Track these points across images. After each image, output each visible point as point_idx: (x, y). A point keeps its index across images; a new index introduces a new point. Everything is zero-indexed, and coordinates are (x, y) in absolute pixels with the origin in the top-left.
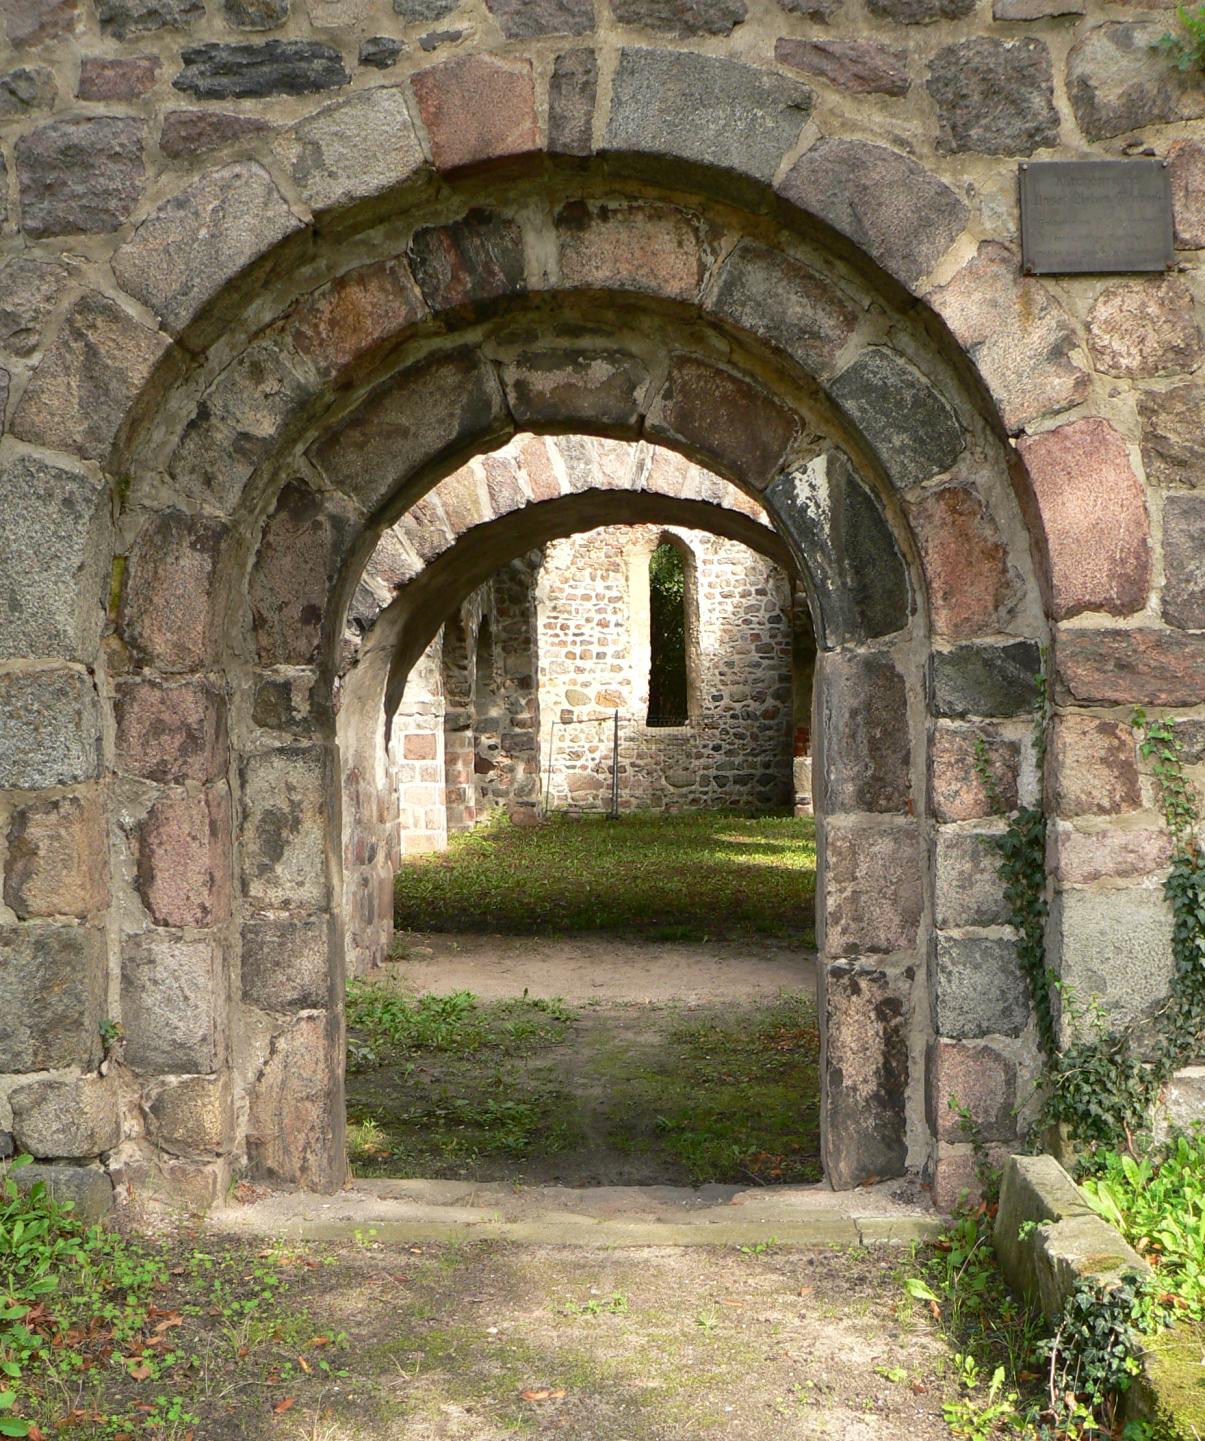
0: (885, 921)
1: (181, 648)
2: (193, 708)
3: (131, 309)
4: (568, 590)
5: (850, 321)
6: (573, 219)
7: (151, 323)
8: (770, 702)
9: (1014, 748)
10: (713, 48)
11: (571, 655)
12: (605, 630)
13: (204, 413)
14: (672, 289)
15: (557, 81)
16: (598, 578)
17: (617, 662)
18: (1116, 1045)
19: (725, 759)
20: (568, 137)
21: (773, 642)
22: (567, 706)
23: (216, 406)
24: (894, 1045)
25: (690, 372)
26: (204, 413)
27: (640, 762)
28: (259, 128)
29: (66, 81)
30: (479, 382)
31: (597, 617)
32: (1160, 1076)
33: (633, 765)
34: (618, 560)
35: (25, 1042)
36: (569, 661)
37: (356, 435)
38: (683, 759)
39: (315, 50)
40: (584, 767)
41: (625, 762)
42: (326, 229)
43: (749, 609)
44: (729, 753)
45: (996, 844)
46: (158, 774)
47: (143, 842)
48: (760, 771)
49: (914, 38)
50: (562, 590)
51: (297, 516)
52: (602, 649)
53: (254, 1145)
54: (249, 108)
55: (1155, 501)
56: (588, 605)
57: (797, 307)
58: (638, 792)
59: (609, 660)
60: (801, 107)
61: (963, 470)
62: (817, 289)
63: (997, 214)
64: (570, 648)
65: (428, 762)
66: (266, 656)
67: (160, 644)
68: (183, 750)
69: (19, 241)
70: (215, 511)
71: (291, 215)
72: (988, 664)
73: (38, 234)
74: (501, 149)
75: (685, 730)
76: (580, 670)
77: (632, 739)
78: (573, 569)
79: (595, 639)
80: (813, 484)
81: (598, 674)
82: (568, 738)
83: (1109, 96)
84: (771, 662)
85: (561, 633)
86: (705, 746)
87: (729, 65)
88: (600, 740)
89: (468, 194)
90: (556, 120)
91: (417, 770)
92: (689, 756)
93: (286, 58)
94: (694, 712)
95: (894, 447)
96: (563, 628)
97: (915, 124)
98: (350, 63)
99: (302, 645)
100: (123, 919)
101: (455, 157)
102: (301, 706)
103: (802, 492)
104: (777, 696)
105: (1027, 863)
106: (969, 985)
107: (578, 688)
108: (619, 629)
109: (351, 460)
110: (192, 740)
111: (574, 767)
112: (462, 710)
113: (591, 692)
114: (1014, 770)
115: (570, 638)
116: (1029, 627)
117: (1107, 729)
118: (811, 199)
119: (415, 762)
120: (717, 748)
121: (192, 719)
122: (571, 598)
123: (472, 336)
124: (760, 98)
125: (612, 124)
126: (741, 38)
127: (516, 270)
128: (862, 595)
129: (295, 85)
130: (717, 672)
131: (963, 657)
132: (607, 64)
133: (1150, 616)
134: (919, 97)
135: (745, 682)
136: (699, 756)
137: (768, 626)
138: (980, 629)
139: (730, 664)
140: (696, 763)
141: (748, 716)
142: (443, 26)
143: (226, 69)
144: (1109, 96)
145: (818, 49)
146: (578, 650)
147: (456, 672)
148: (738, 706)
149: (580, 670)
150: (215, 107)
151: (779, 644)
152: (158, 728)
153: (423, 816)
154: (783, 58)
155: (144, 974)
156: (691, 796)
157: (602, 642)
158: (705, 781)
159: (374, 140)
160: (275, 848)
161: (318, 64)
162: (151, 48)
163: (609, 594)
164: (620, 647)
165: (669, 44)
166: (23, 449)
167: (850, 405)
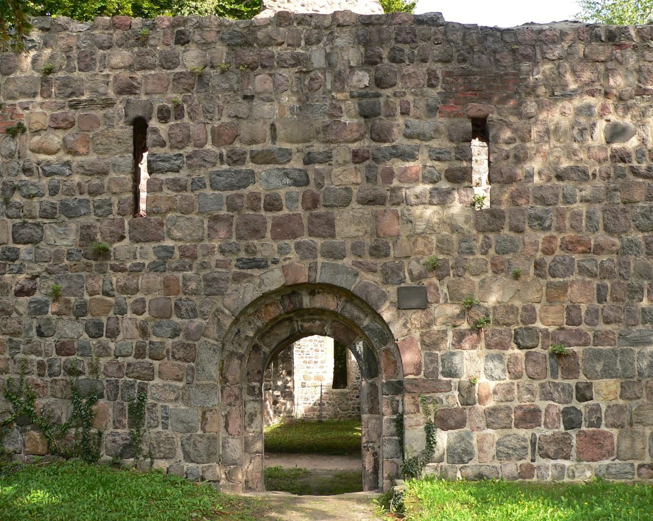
0: (374, 436)
1: (235, 379)
2: (237, 392)
3: (227, 312)
5: (366, 316)
6: (312, 293)
7: (231, 314)
9: (398, 401)
10: (340, 262)
11: (305, 362)
13: (239, 331)
14: (332, 308)
15: (310, 268)
17: (321, 365)
18: (415, 458)
20: (312, 280)
23: (241, 330)
24: (376, 462)
25: (335, 323)
26: (239, 331)
28: (252, 276)
29: (213, 264)
30: (293, 325)
32: (424, 465)
35: (205, 457)
37: (268, 335)
38: (346, 401)
39: (263, 260)
41: (325, 402)
42: (265, 296)
45: (394, 420)
46: (230, 405)
47: (226, 418)
49: (378, 261)
51: (256, 351)
52: (316, 360)
53: (246, 482)
54: (250, 271)
55: (423, 353)
56: (311, 343)
57: (356, 313)
58: (330, 413)
59: (319, 364)
60: (356, 275)
61: (388, 346)
62: (360, 309)
63: (393, 297)
64: (305, 359)
66: (250, 381)
67: (230, 378)
68: (235, 400)
69: (204, 296)
70: (241, 351)
71: (258, 294)
72: (393, 385)
73: (208, 295)
74: (299, 282)
75: (346, 390)
76: (308, 367)
80: (360, 347)
83: (415, 273)
87: (343, 266)
89: (291, 291)
90: (309, 276)
92: (347, 400)
93: (257, 261)
94: (350, 383)
95: (375, 341)
97: (378, 278)
98: (269, 263)
99: (257, 378)
100: (222, 434)
101: (290, 283)
102: (257, 391)
103: (358, 349)
105: (399, 424)
106: (388, 449)
109: (267, 340)
110: (237, 398)
113: (312, 376)
114: (398, 406)
115: (305, 356)
116: (400, 378)
117: (413, 398)
118: (358, 294)
121: (237, 394)
123: (292, 315)
124: (348, 273)
126: (345, 260)
127: (301, 304)
128: (369, 370)
129: (259, 267)
131: (388, 383)
132: (319, 265)
133: (422, 376)
134: (379, 273)
136: (351, 400)
138: (391, 378)
140: (350, 402)
142: (288, 256)
143: (244, 263)
144: (415, 273)
145: (360, 263)
149: (308, 367)
150: (243, 271)
152: (230, 395)
154: (353, 265)
155: (227, 445)
157: (316, 357)
158: (353, 409)
159: (274, 279)
160: (252, 421)
161: (263, 263)
162: (230, 258)
164: (322, 359)
165: (331, 261)
166: (205, 339)
167: (366, 333)
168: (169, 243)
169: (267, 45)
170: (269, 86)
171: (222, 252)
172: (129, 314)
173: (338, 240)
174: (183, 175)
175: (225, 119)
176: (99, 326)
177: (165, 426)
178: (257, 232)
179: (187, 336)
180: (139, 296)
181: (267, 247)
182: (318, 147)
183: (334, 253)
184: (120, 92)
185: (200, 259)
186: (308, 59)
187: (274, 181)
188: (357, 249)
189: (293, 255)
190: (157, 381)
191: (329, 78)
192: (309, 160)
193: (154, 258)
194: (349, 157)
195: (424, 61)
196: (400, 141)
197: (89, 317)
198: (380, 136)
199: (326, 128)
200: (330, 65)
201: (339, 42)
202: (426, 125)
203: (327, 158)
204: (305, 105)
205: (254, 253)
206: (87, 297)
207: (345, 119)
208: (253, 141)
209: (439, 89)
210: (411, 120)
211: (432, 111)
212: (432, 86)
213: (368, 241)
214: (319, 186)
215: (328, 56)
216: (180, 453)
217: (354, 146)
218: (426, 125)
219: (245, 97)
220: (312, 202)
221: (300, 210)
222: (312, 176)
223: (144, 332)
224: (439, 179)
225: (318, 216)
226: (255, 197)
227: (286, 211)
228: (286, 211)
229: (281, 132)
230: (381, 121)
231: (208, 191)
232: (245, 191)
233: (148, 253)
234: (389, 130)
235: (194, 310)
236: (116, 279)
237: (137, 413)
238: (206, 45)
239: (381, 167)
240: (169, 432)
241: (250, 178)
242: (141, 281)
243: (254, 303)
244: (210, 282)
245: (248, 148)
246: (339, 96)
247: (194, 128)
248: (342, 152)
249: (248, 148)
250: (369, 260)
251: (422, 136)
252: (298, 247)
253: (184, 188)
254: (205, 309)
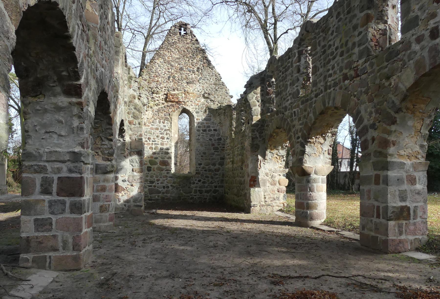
4: (151, 126)
8: (217, 166)
12: (163, 140)
16: (161, 123)
19: (202, 184)
21: (218, 146)
22: (150, 166)
27: (174, 185)
31: (161, 136)
33: (171, 186)
34: (168, 117)
36: (150, 150)
40: (155, 186)
41: (169, 185)
43: (212, 135)
44: (204, 183)
48: (214, 188)
50: (149, 126)
56: (158, 132)
58: (173, 195)
64: (151, 146)
65: (77, 199)
77: (171, 177)
78: (153, 119)
79: (159, 143)
81: (160, 155)
82: (149, 176)
84: (218, 153)
85: (148, 141)
86: (196, 180)
88: (161, 177)
91: (68, 205)
96: (149, 139)
104: (220, 164)
107: (153, 159)
108: (168, 140)
111: (151, 186)
112: (109, 163)
115: (151, 142)
119: (66, 199)
120: (200, 181)
122: (152, 129)
130: (200, 155)
135: (209, 159)
136: (194, 183)
137: (217, 141)
139: (204, 153)
140: (192, 185)
141: (210, 170)
146: (154, 146)
147: (107, 142)
148: (207, 167)
151: (221, 147)
153: (70, 240)
156: (191, 197)
158: (196, 192)
163: (165, 128)
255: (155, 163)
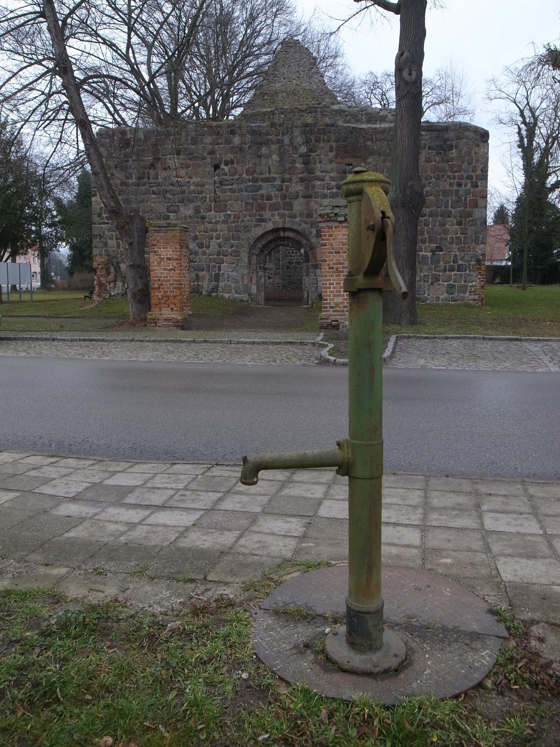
24: (308, 295)
42: (266, 232)
57: (301, 238)
89: (276, 230)
97: (309, 226)
125: (287, 225)
159: (270, 226)
168: (229, 212)
169: (266, 135)
170: (267, 152)
171: (250, 216)
172: (214, 240)
173: (294, 211)
174: (234, 186)
175: (251, 165)
176: (202, 244)
177: (228, 281)
178: (263, 208)
179: (237, 248)
180: (218, 232)
181: (267, 214)
182: (287, 176)
183: (293, 216)
184: (209, 154)
185: (241, 219)
186: (283, 141)
187: (270, 189)
188: (301, 215)
189: (277, 217)
190: (225, 264)
191: (291, 149)
192: (283, 181)
193: (223, 218)
194: (298, 180)
195: (329, 141)
196: (318, 174)
197: (198, 241)
198: (311, 172)
199: (290, 168)
200: (292, 144)
201: (295, 134)
202: (329, 167)
203: (290, 180)
204: (281, 160)
205: (262, 216)
206: (198, 233)
207: (297, 165)
208: (261, 174)
209: (334, 153)
210: (322, 165)
211: (331, 161)
212: (331, 152)
213: (306, 212)
214: (287, 191)
215: (290, 140)
216: (234, 291)
217: (300, 176)
218: (329, 167)
219: (258, 156)
220: (284, 197)
221: (279, 200)
222: (284, 187)
223: (220, 246)
224: (333, 188)
225: (286, 203)
226: (262, 195)
227: (274, 201)
228: (274, 201)
229: (272, 170)
230: (311, 166)
231: (244, 193)
232: (258, 193)
233: (221, 217)
234: (314, 169)
235: (239, 238)
236: (209, 226)
237: (217, 278)
238: (242, 135)
239: (310, 184)
240: (229, 283)
241: (260, 188)
242: (219, 227)
243: (262, 235)
244: (246, 227)
245: (260, 176)
246: (295, 156)
247: (239, 168)
248: (295, 179)
249: (260, 176)
250: (305, 219)
251: (326, 172)
252: (279, 214)
253: (235, 192)
254: (243, 237)
255: (292, 263)
